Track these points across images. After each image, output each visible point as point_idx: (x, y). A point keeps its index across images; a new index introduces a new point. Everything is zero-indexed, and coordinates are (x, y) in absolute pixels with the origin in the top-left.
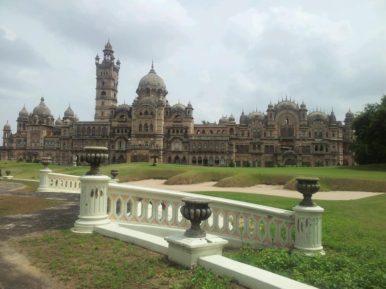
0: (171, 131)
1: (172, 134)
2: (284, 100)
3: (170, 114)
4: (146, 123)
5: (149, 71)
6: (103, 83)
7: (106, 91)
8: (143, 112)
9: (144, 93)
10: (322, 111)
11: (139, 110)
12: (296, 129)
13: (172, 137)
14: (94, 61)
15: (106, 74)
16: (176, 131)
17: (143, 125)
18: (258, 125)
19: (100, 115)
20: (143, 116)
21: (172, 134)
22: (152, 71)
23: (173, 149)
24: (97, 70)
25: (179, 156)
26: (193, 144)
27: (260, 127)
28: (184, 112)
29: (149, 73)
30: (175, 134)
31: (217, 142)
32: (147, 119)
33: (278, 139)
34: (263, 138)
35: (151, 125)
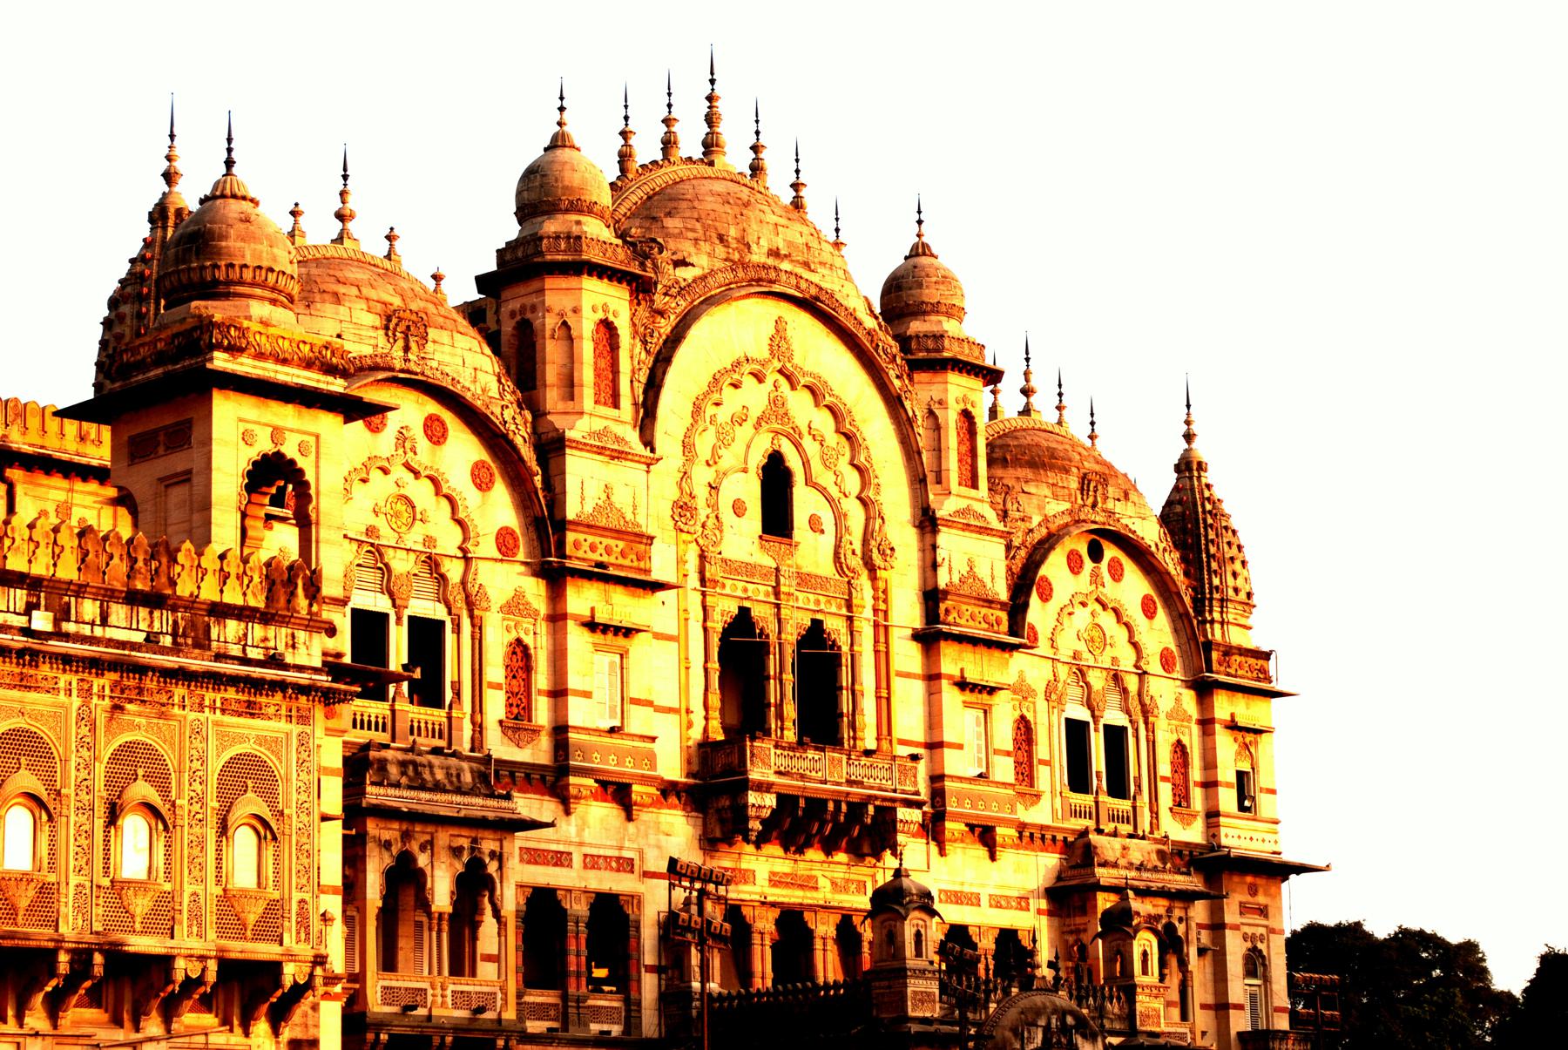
2: (690, 144)
10: (1077, 428)
12: (883, 656)
18: (421, 492)
27: (448, 540)
31: (139, 726)
33: (713, 789)
34: (499, 747)
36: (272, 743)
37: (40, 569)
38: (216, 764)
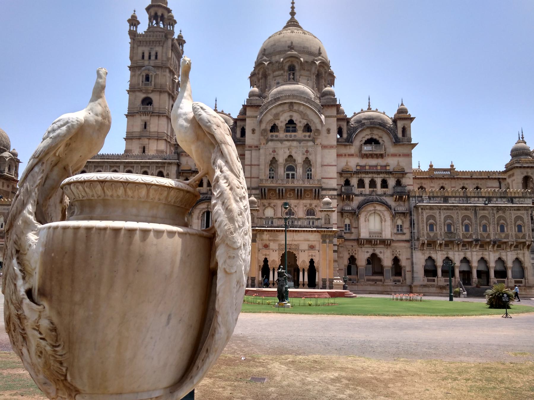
0: (354, 181)
1: (356, 191)
3: (350, 135)
4: (290, 156)
5: (285, 25)
6: (147, 78)
7: (155, 97)
8: (281, 123)
9: (277, 73)
11: (269, 117)
13: (356, 201)
14: (127, 26)
15: (153, 57)
16: (367, 182)
17: (281, 159)
19: (137, 151)
20: (282, 134)
21: (356, 191)
22: (293, 23)
23: (364, 234)
24: (132, 49)
25: (381, 256)
26: (428, 218)
28: (389, 129)
29: (285, 27)
30: (367, 190)
31: (501, 213)
32: (295, 144)
35: (307, 162)
36: (523, 214)
37: (487, 195)
38: (513, 217)
